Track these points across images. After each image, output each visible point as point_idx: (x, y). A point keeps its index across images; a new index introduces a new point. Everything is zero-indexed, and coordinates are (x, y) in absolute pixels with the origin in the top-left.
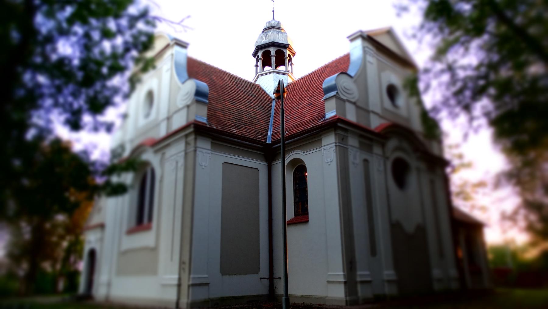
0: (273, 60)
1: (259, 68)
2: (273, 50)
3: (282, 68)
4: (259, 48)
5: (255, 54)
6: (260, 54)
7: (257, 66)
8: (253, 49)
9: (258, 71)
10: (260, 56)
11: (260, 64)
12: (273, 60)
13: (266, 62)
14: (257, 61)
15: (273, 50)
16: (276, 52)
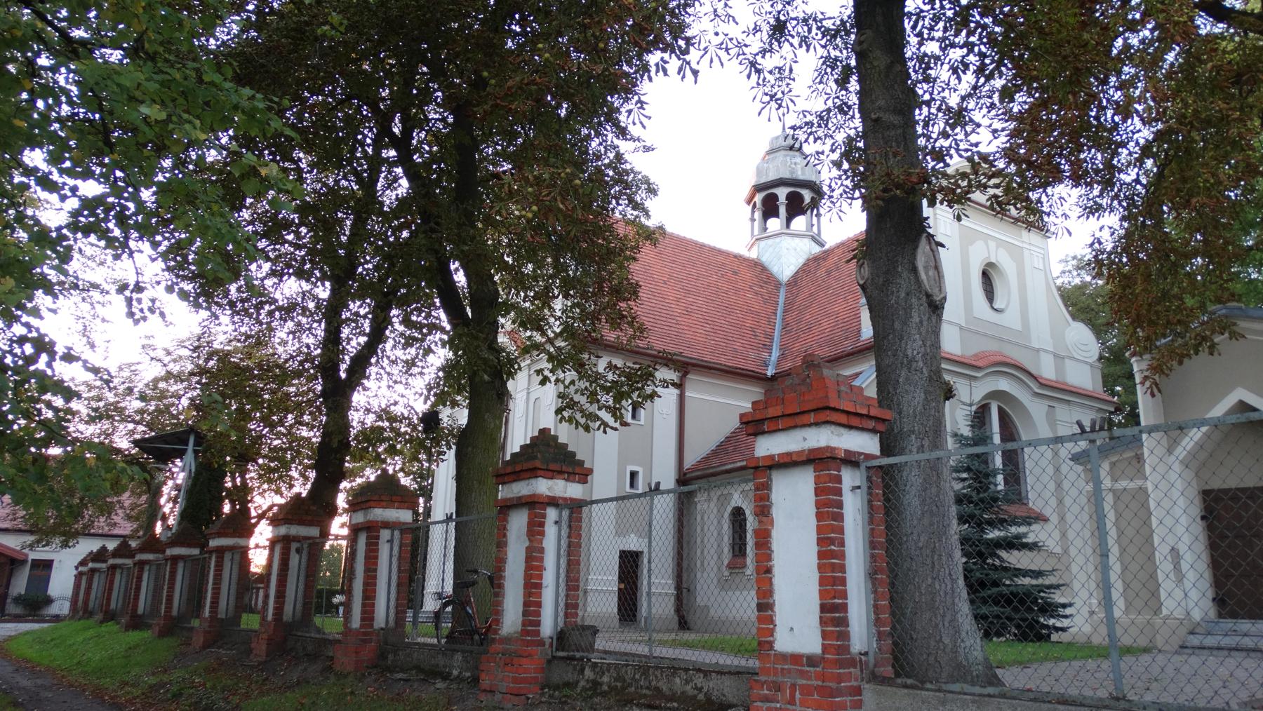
0: (782, 210)
1: (756, 224)
2: (782, 193)
3: (799, 223)
4: (758, 188)
5: (749, 200)
6: (758, 198)
7: (753, 220)
8: (746, 191)
9: (756, 232)
10: (759, 205)
11: (758, 215)
12: (782, 210)
13: (770, 209)
14: (753, 212)
15: (782, 193)
16: (789, 197)
